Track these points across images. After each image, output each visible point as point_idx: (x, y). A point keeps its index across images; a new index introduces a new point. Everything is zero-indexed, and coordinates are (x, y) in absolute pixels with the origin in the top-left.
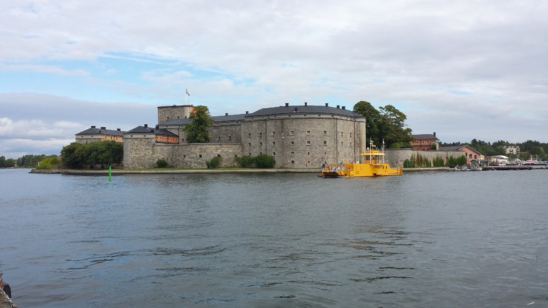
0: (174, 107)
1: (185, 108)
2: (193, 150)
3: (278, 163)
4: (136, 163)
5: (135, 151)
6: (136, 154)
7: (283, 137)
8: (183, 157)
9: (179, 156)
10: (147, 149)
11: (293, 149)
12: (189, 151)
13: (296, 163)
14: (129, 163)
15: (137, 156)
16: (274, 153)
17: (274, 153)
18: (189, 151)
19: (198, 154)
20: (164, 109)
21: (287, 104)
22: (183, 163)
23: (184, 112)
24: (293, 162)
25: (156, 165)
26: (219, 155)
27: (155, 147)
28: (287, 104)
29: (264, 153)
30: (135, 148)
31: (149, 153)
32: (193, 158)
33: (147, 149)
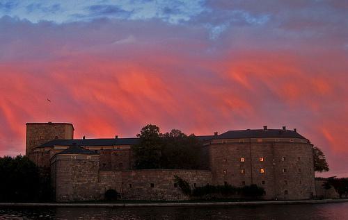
0: (50, 123)
1: (67, 126)
2: (166, 178)
3: (269, 193)
4: (78, 194)
5: (78, 177)
6: (78, 182)
7: (274, 164)
8: (150, 186)
9: (141, 184)
10: (92, 175)
11: (285, 178)
12: (161, 178)
13: (290, 193)
14: (69, 193)
15: (80, 183)
16: (263, 183)
17: (263, 183)
18: (161, 178)
19: (173, 183)
20: (37, 126)
21: (265, 127)
22: (150, 193)
23: (64, 131)
24: (286, 192)
25: (102, 197)
26: (195, 184)
27: (101, 173)
28: (265, 127)
29: (248, 183)
30: (78, 173)
31: (94, 180)
32: (165, 187)
33: (92, 175)
